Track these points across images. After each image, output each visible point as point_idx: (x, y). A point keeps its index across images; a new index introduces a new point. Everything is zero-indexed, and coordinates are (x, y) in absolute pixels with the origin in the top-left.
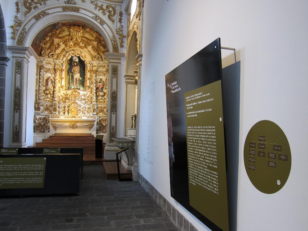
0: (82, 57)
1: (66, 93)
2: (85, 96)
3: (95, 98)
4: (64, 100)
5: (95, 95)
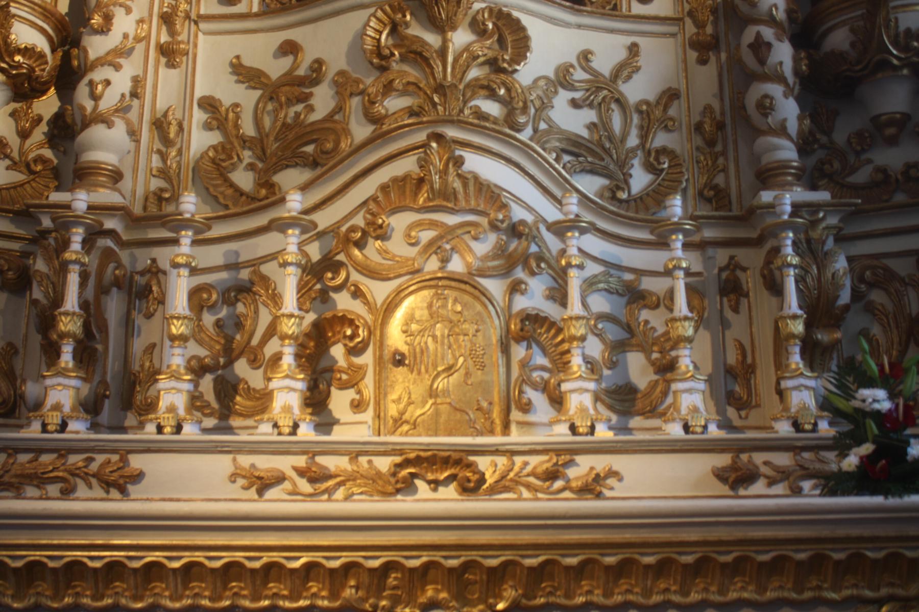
1: (276, 68)
2: (601, 92)
3: (789, 110)
4: (244, 179)
5: (783, 54)
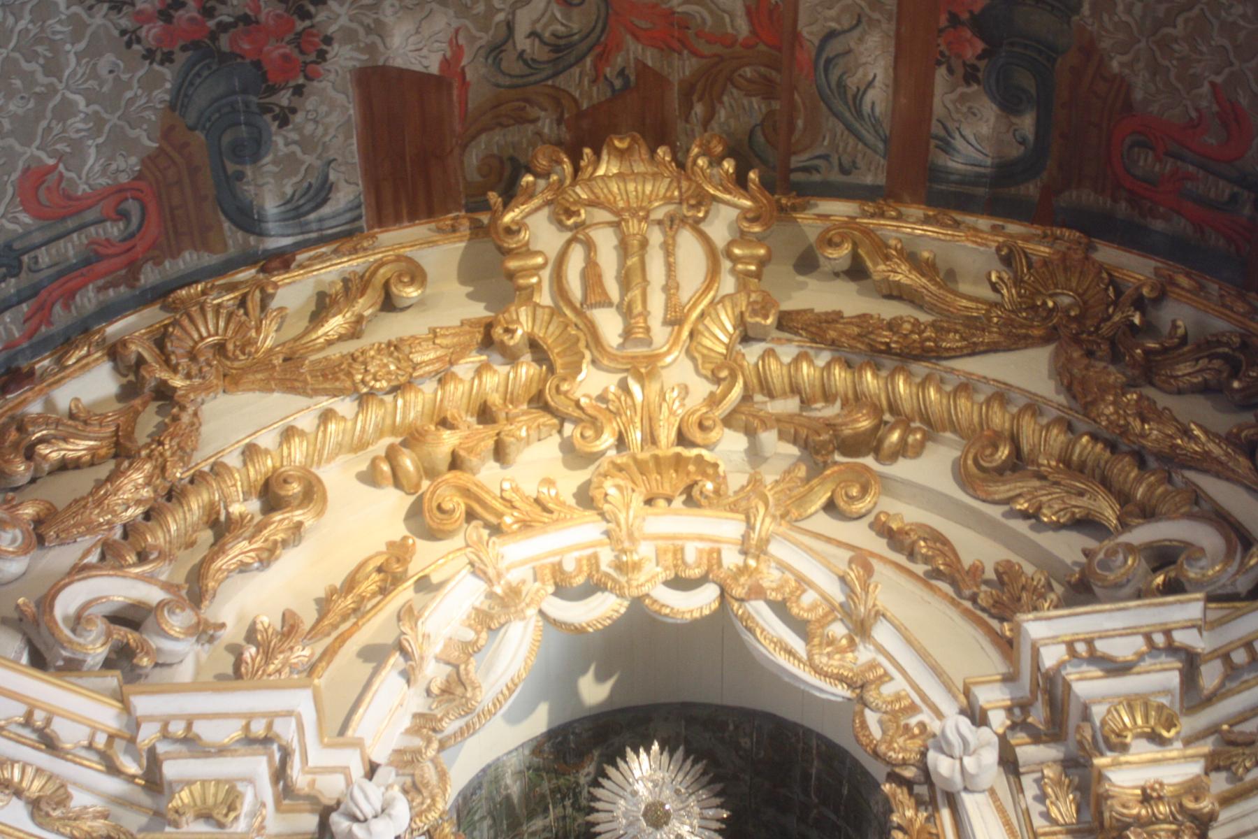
0: (781, 609)
